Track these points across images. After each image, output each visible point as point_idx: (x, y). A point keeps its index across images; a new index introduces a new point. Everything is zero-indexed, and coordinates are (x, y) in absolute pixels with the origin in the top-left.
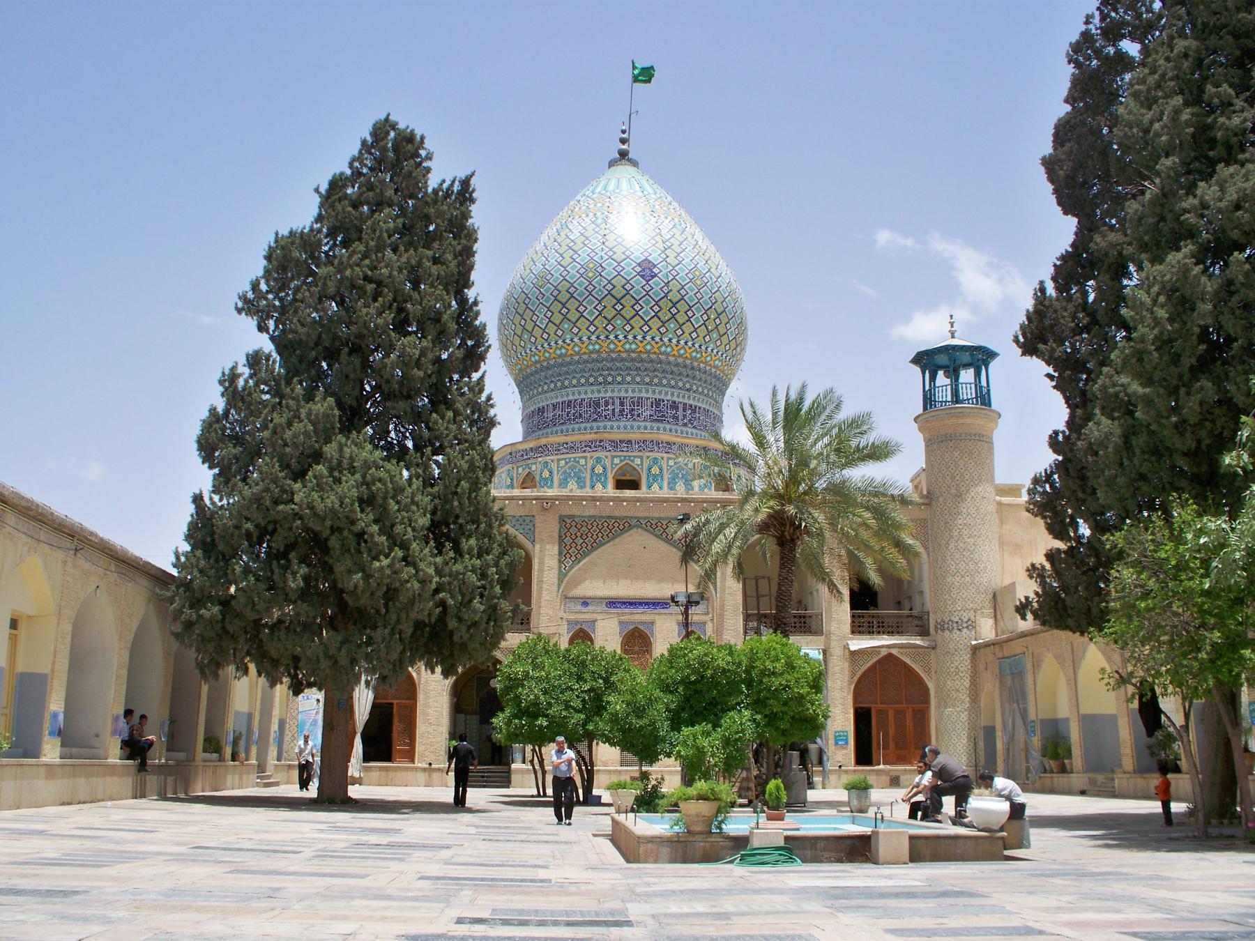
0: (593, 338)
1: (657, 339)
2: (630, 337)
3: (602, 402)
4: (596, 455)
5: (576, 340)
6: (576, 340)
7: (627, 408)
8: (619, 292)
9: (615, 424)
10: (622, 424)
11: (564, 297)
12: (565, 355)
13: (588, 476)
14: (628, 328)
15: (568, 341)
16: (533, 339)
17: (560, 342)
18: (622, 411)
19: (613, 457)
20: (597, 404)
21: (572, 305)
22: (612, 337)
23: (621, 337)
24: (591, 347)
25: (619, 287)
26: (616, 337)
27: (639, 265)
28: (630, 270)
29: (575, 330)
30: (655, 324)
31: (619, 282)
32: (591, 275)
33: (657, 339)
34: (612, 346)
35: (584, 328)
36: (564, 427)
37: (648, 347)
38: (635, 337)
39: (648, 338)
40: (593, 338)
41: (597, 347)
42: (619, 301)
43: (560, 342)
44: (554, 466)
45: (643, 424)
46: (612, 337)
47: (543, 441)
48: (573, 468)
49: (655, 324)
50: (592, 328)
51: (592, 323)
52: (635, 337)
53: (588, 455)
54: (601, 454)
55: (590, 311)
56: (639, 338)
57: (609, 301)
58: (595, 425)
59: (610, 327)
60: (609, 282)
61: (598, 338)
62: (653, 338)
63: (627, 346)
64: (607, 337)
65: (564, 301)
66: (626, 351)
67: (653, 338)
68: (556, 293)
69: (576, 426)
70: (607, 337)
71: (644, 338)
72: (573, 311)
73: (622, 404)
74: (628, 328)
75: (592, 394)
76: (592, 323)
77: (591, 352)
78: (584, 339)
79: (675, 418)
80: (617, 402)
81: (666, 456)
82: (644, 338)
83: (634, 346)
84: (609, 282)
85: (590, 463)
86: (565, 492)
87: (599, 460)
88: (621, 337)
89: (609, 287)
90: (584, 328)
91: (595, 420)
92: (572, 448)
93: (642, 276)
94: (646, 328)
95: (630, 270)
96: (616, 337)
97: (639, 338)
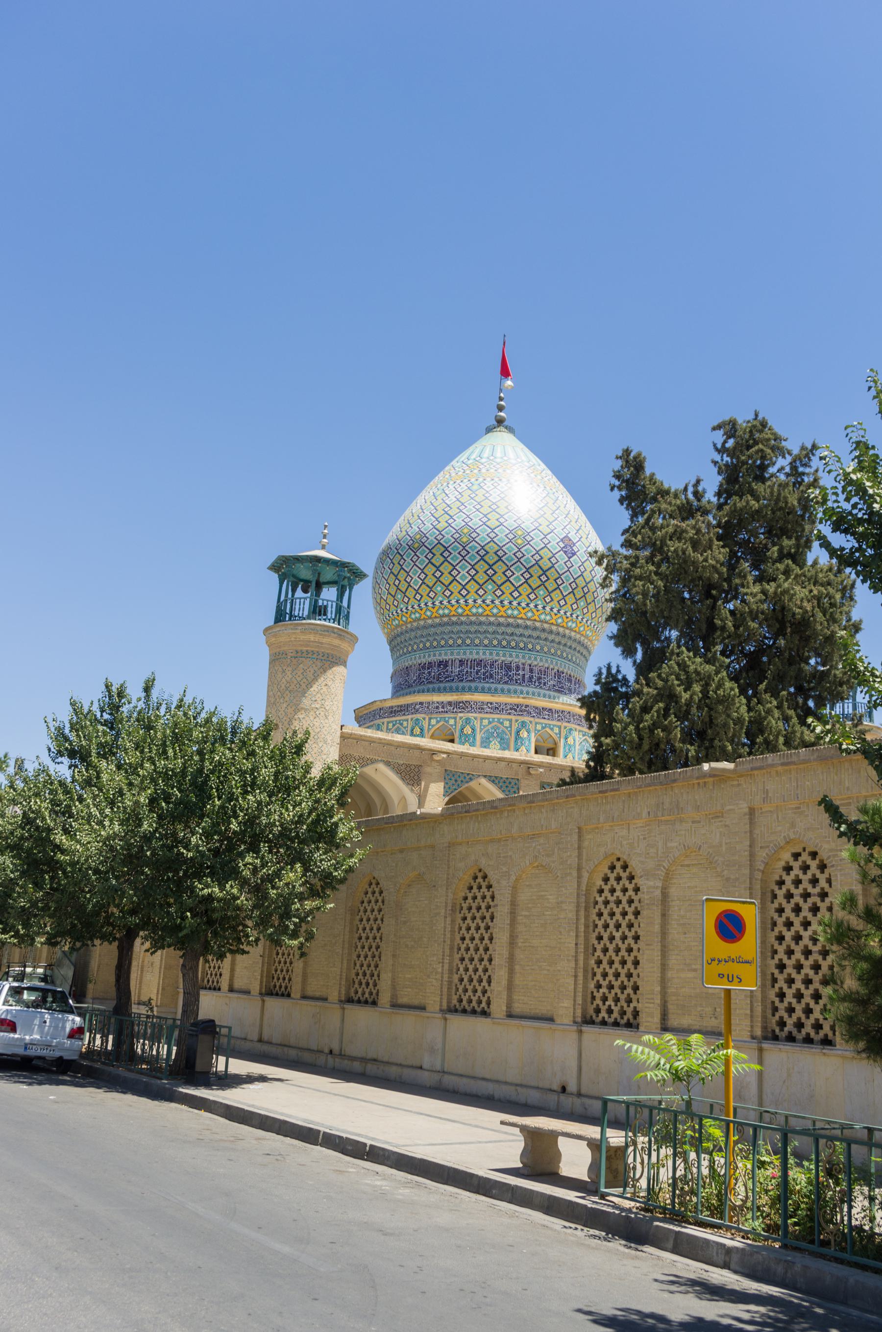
0: (515, 603)
1: (568, 614)
2: (548, 609)
3: (513, 665)
4: (521, 719)
5: (497, 602)
6: (497, 602)
7: (535, 675)
8: (545, 564)
9: (525, 689)
10: (531, 690)
11: (491, 558)
12: (481, 615)
13: (513, 739)
14: (548, 599)
15: (488, 602)
16: (447, 593)
17: (479, 601)
18: (531, 678)
19: (536, 723)
20: (509, 667)
21: (500, 568)
22: (532, 605)
23: (540, 607)
24: (510, 612)
25: (546, 559)
26: (536, 606)
27: (562, 540)
28: (555, 545)
29: (499, 593)
30: (570, 599)
31: (545, 554)
32: (520, 541)
33: (568, 614)
34: (530, 614)
35: (507, 592)
36: (473, 685)
37: (560, 621)
38: (551, 609)
39: (562, 612)
40: (515, 603)
41: (516, 612)
42: (544, 572)
43: (479, 601)
44: (477, 725)
45: (547, 692)
46: (532, 605)
47: (467, 697)
48: (495, 728)
49: (570, 599)
50: (516, 594)
51: (516, 589)
52: (551, 609)
53: (513, 718)
54: (527, 719)
55: (517, 578)
56: (555, 610)
57: (536, 571)
58: (506, 687)
59: (532, 596)
60: (537, 552)
61: (519, 604)
62: (565, 613)
63: (543, 617)
64: (527, 605)
65: (491, 563)
66: (541, 621)
67: (565, 613)
68: (482, 553)
69: (487, 685)
70: (527, 605)
71: (559, 611)
72: (500, 573)
73: (531, 671)
74: (548, 599)
75: (503, 657)
76: (516, 589)
77: (509, 617)
78: (506, 603)
79: (570, 690)
80: (527, 668)
81: (578, 727)
82: (559, 611)
83: (548, 618)
84: (537, 552)
85: (515, 726)
86: (486, 752)
87: (523, 724)
88: (540, 607)
89: (537, 557)
90: (507, 592)
91: (506, 683)
92: (497, 708)
93: (565, 552)
94: (562, 602)
95: (555, 545)
96: (536, 606)
97: (555, 610)
